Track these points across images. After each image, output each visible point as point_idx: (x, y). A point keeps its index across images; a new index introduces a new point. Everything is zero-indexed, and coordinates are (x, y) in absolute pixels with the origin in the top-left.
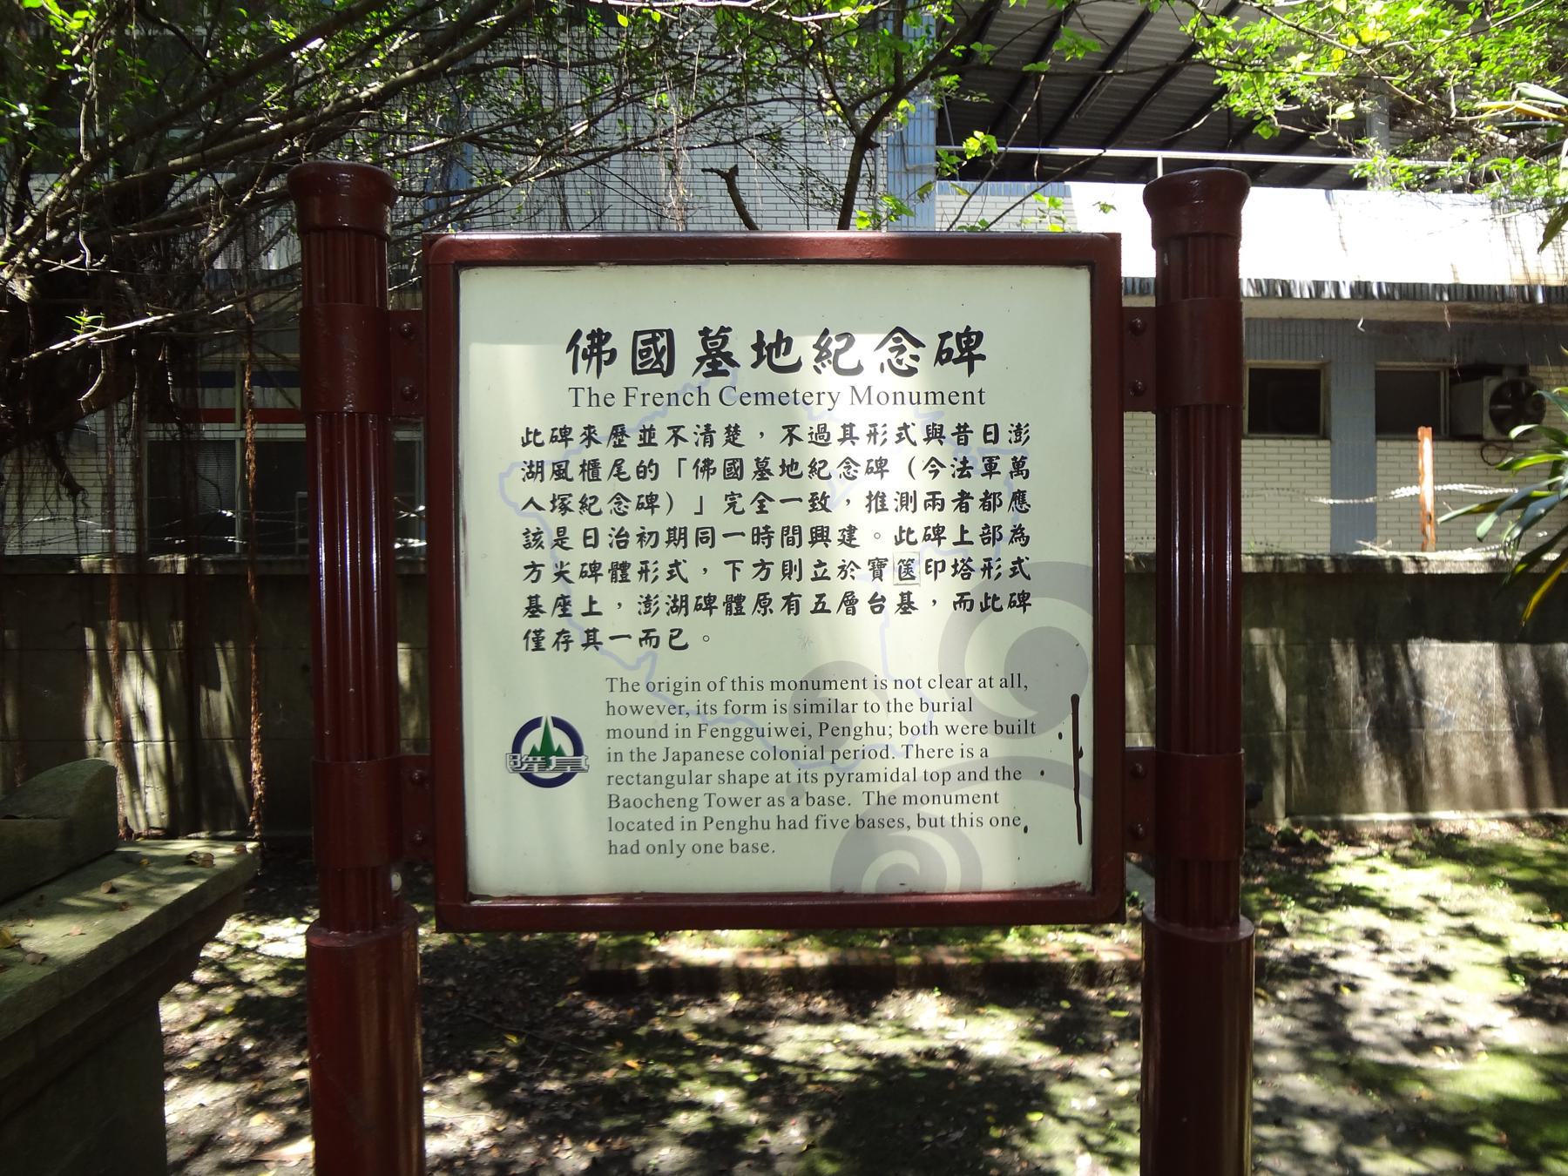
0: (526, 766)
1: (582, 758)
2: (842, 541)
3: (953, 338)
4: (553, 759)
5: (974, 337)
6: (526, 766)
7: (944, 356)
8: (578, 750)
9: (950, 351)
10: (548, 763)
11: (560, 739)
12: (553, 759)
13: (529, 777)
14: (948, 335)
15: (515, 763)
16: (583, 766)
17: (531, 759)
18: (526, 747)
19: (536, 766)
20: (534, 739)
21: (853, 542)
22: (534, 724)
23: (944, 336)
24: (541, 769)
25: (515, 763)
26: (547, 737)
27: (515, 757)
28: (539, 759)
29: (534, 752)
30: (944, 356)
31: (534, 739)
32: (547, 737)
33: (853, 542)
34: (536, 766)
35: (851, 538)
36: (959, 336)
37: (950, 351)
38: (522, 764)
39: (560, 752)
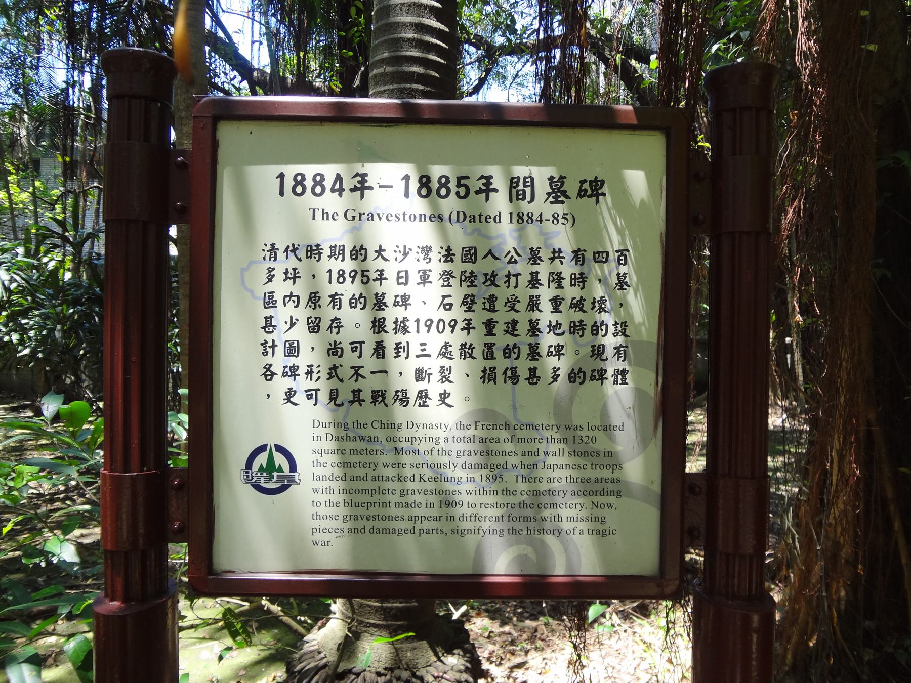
0: (255, 479)
1: (296, 474)
2: (507, 332)
3: (588, 183)
4: (275, 474)
5: (599, 183)
6: (255, 479)
7: (582, 193)
8: (293, 468)
9: (586, 190)
10: (272, 477)
11: (280, 460)
12: (275, 474)
13: (258, 487)
14: (585, 181)
15: (248, 477)
16: (296, 480)
17: (259, 474)
18: (256, 466)
19: (262, 479)
20: (262, 460)
21: (516, 333)
22: (262, 448)
23: (582, 182)
24: (266, 482)
25: (248, 477)
26: (271, 458)
27: (248, 473)
28: (265, 474)
29: (261, 469)
30: (582, 193)
31: (262, 460)
32: (271, 458)
33: (516, 333)
34: (262, 479)
35: (514, 329)
36: (591, 182)
37: (586, 190)
38: (252, 478)
39: (280, 469)
